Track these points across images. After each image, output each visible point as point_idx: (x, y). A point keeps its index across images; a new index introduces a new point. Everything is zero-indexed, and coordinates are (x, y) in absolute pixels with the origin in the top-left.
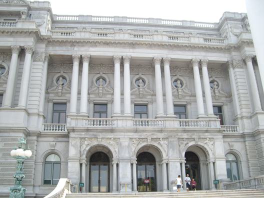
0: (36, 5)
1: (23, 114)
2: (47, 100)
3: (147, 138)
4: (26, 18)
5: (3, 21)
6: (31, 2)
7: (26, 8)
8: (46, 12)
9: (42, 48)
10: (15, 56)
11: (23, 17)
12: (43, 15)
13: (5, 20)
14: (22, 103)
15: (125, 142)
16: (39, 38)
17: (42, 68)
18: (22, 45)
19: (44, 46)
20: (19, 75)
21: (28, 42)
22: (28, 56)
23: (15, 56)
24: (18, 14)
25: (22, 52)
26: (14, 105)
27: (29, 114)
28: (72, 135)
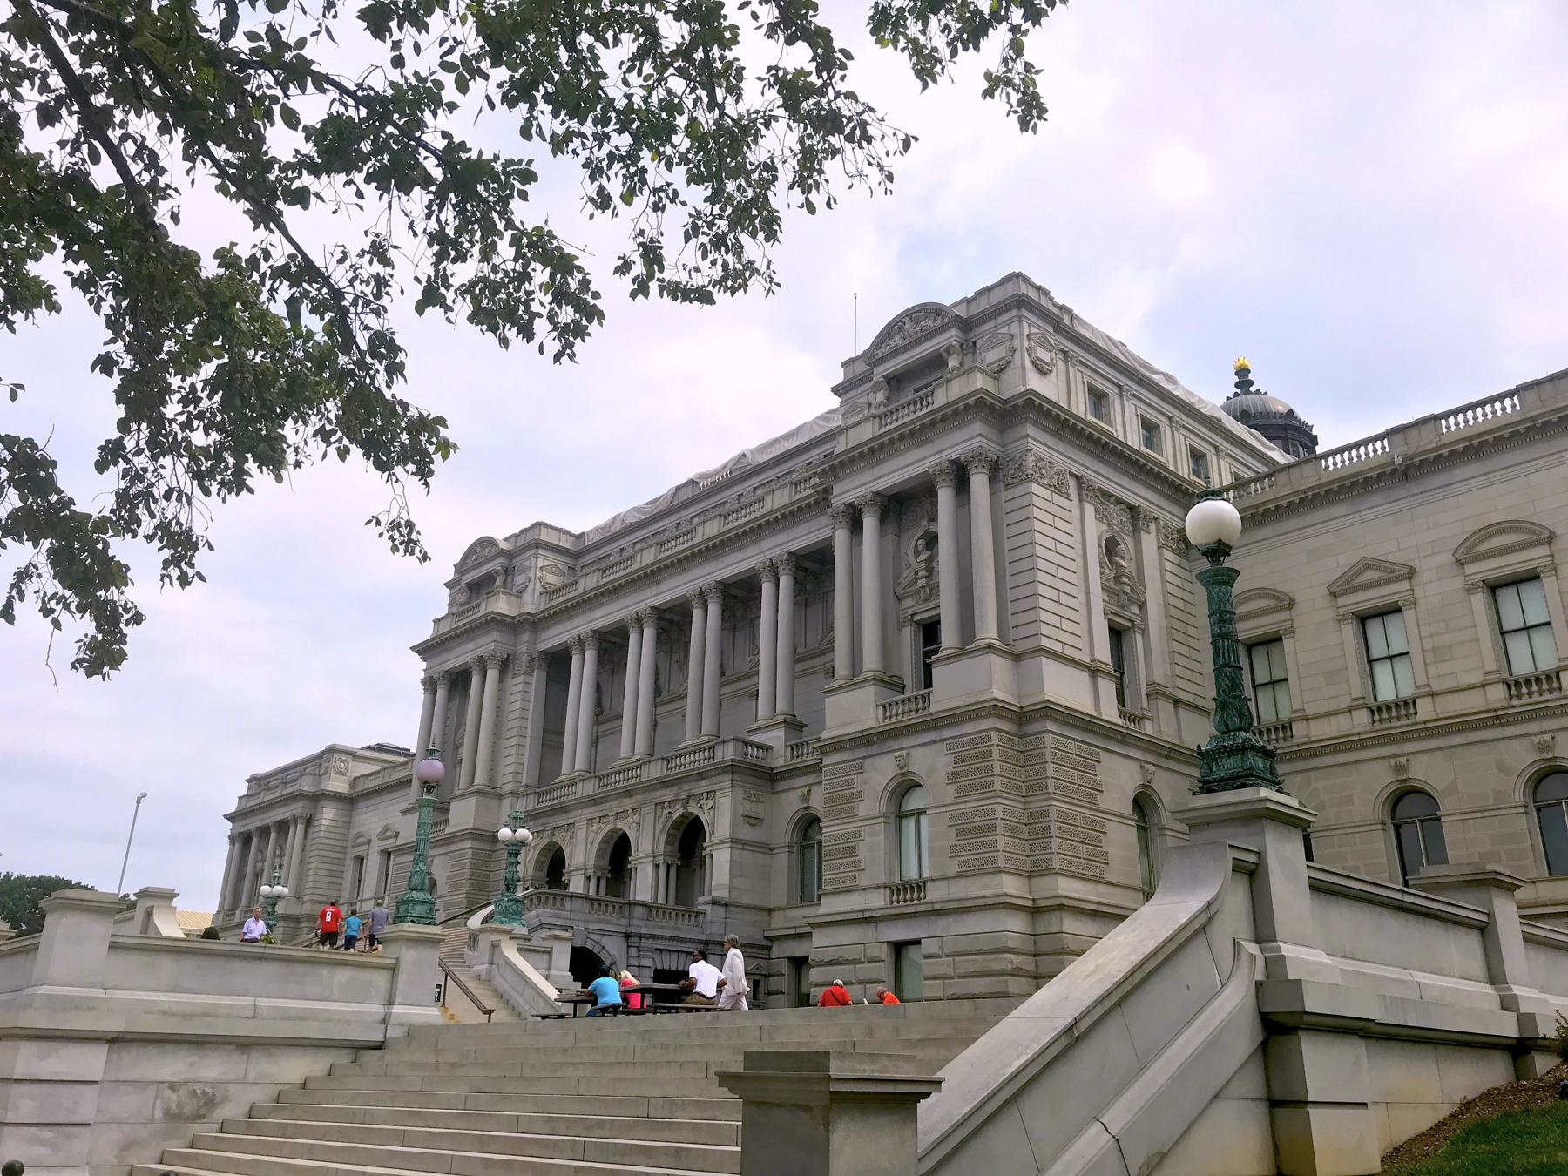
0: (983, 305)
4: (961, 364)
5: (912, 396)
6: (968, 301)
7: (954, 331)
8: (1014, 313)
10: (945, 496)
11: (953, 362)
12: (1004, 330)
13: (916, 391)
18: (954, 453)
22: (979, 482)
23: (945, 496)
24: (936, 362)
25: (960, 475)
27: (1017, 657)
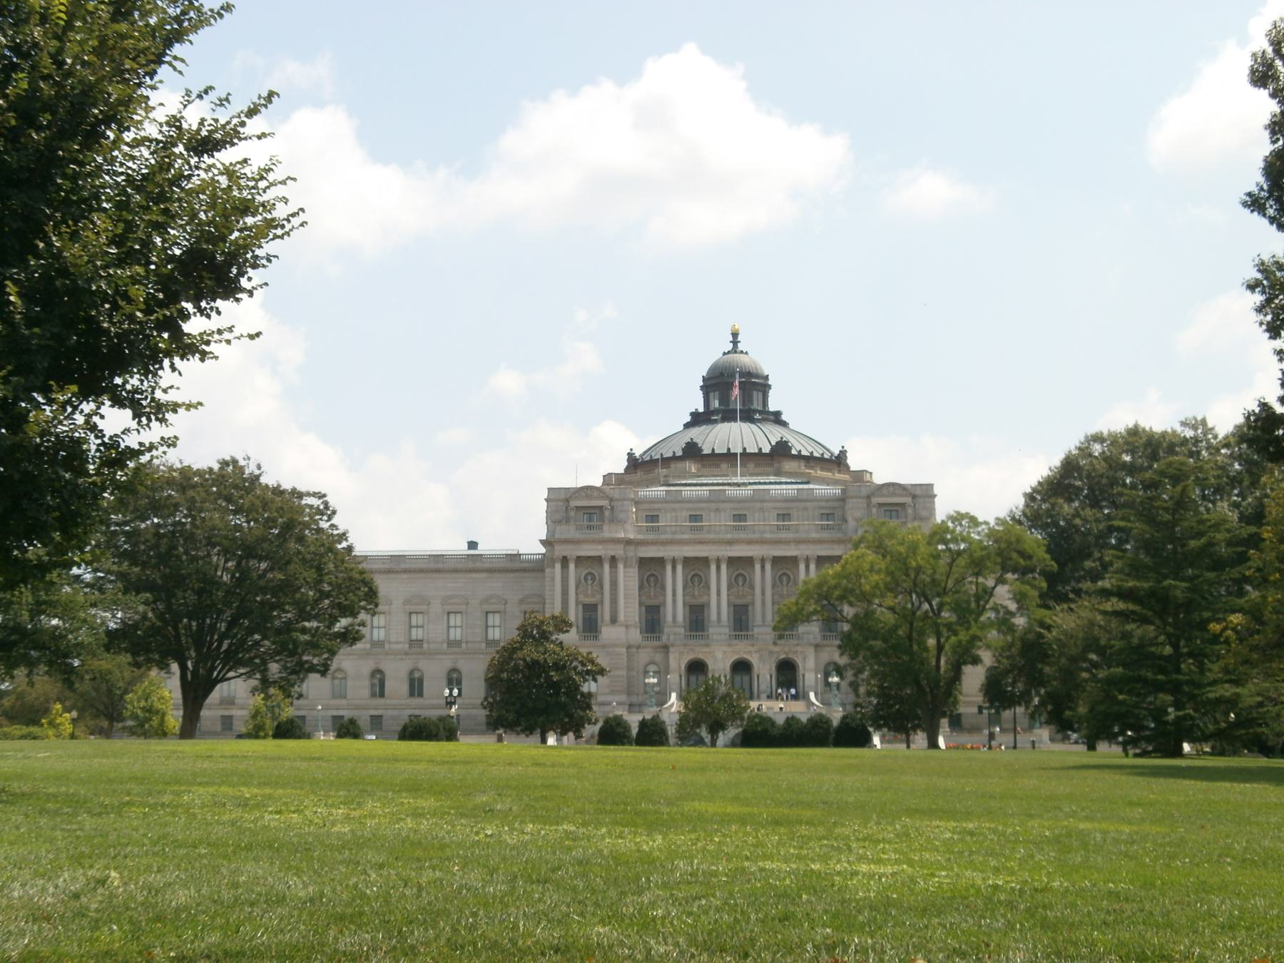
1: (623, 629)
2: (640, 604)
3: (743, 650)
9: (631, 552)
14: (621, 617)
15: (719, 655)
16: (628, 542)
17: (634, 572)
19: (632, 548)
20: (614, 584)
21: (618, 551)
22: (621, 566)
23: (607, 567)
25: (613, 560)
26: (614, 620)
28: (672, 649)
